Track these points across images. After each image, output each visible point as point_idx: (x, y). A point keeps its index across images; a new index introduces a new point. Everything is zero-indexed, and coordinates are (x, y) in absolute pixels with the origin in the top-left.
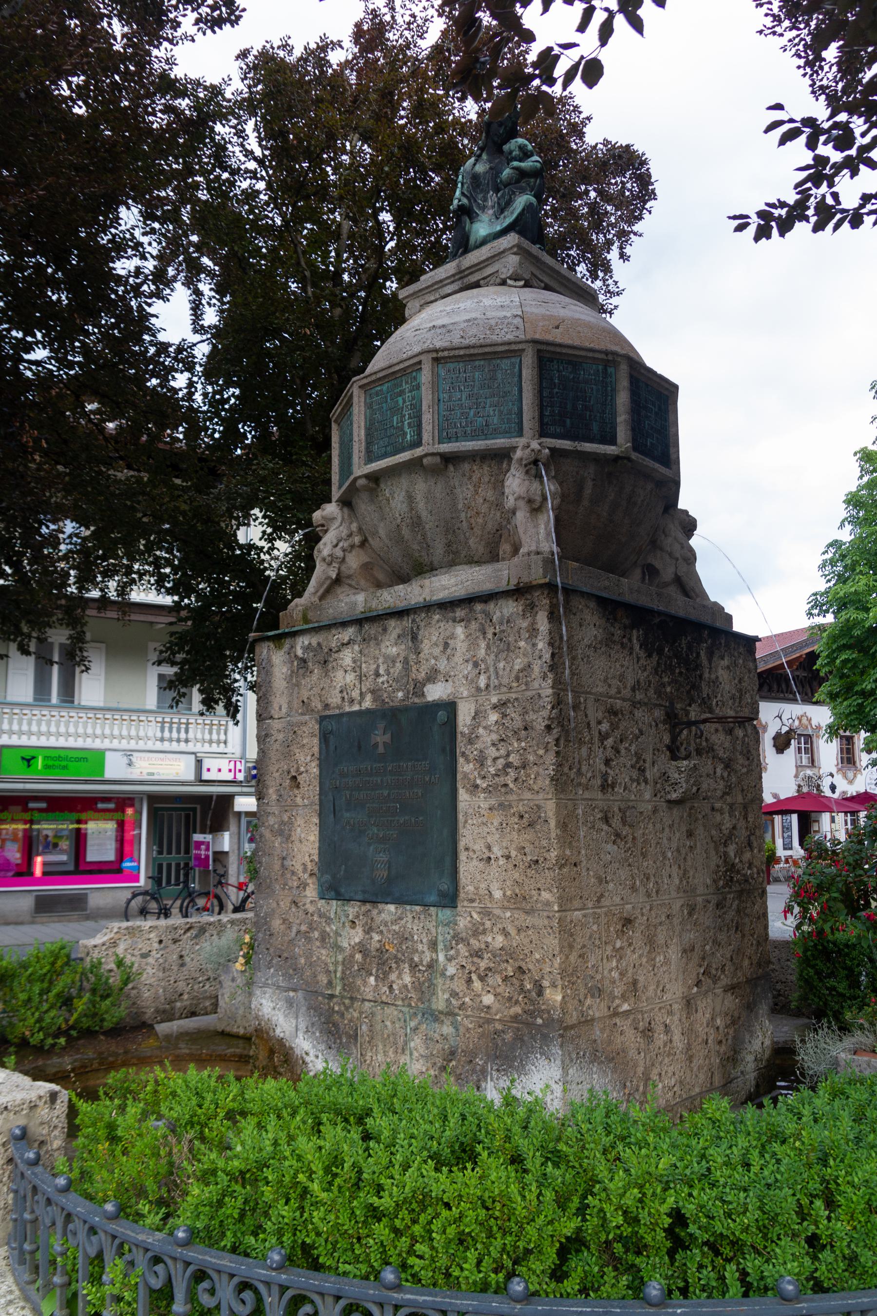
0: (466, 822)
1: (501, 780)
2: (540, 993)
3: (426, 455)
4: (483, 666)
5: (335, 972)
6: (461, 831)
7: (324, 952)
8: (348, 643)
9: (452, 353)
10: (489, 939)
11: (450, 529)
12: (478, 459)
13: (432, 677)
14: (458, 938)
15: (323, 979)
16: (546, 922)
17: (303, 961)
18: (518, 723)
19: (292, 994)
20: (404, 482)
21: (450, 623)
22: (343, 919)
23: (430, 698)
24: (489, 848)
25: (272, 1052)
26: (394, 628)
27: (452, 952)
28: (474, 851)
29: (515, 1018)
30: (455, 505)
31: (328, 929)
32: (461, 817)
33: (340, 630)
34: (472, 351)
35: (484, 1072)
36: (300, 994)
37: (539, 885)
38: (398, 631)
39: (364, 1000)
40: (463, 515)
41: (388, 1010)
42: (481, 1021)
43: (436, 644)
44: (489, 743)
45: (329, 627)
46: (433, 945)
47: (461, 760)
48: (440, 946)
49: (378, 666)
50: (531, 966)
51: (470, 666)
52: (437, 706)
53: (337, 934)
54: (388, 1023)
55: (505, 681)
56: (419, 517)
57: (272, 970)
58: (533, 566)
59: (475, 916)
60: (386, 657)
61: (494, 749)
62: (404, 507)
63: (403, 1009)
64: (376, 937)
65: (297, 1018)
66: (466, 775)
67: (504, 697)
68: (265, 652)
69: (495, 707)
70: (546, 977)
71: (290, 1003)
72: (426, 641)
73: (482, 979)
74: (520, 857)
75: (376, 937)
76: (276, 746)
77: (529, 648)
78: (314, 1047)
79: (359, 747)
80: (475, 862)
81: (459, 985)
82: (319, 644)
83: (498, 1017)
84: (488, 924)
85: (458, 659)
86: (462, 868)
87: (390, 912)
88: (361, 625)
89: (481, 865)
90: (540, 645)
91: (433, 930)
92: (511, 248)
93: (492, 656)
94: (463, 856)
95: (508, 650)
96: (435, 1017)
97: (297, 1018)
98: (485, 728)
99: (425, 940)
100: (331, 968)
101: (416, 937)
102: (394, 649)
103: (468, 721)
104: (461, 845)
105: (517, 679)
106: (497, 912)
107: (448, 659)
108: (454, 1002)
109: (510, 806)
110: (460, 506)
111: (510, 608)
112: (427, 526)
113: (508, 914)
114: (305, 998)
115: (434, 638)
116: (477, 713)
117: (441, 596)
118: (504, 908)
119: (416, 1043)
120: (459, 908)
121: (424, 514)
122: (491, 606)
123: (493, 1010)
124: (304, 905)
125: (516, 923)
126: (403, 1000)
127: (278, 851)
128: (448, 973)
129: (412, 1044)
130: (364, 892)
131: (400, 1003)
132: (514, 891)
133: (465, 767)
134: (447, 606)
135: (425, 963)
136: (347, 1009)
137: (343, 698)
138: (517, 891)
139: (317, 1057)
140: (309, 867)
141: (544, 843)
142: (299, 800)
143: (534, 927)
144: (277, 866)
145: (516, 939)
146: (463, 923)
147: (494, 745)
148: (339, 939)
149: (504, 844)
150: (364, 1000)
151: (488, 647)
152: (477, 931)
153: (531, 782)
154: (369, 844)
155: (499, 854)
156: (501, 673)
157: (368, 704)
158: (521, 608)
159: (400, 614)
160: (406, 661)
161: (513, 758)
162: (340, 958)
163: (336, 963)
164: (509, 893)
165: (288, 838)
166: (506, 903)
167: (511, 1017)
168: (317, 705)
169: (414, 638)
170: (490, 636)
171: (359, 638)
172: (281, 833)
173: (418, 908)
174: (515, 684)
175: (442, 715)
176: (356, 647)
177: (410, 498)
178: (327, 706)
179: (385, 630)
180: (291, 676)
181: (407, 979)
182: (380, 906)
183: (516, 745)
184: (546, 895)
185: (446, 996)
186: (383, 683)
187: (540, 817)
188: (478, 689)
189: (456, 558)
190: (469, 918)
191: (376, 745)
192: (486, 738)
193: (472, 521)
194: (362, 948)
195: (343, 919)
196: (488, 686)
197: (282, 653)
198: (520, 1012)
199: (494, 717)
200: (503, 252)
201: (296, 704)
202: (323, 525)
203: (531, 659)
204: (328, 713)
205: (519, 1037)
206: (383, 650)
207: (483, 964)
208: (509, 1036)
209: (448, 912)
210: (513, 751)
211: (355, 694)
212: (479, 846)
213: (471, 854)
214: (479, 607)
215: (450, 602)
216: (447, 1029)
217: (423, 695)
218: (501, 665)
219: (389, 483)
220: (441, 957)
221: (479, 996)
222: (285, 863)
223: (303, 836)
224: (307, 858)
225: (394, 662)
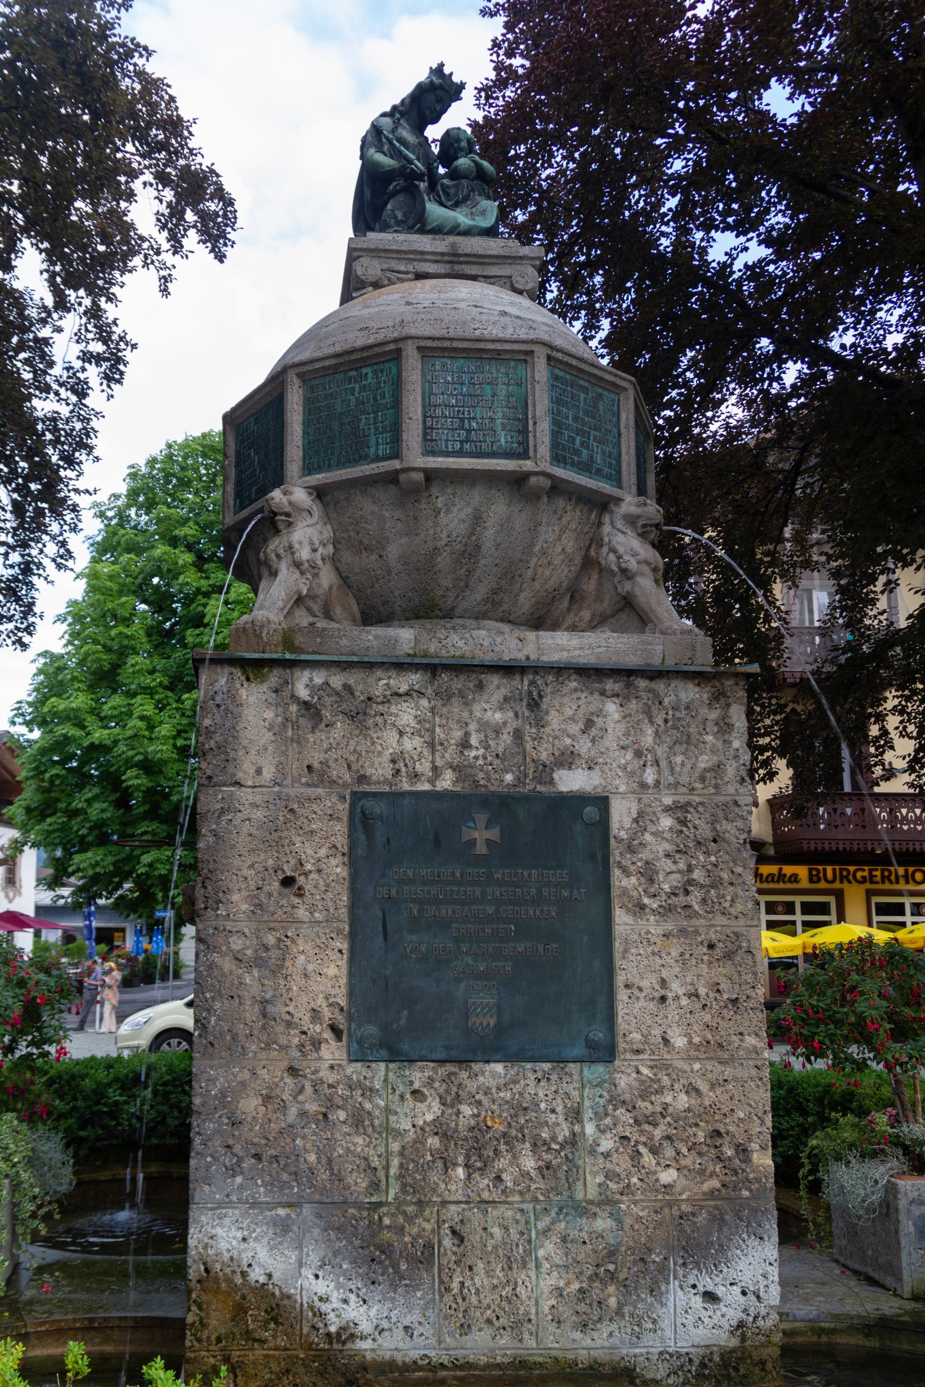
0: (626, 951)
1: (682, 900)
2: (747, 1160)
3: (537, 474)
4: (649, 757)
5: (387, 1168)
6: (618, 962)
7: (359, 1140)
8: (407, 694)
9: (566, 359)
10: (669, 1099)
11: (510, 574)
12: (574, 499)
13: (567, 759)
14: (616, 1101)
15: (359, 1182)
16: (754, 1072)
17: (312, 1158)
18: (705, 832)
19: (281, 1212)
20: (477, 496)
21: (596, 696)
22: (401, 1088)
23: (563, 788)
24: (663, 983)
25: (240, 1310)
26: (498, 687)
27: (608, 1121)
28: (640, 989)
29: (711, 1194)
30: (531, 545)
31: (368, 1106)
32: (618, 946)
33: (393, 673)
34: (583, 366)
35: (662, 1269)
36: (307, 1210)
37: (742, 1029)
38: (503, 691)
39: (444, 1203)
40: (534, 561)
41: (493, 1212)
42: (658, 1205)
43: (572, 719)
44: (661, 854)
45: (370, 666)
46: (575, 1115)
47: (616, 873)
48: (588, 1114)
49: (467, 734)
50: (732, 1128)
51: (629, 755)
52: (578, 800)
53: (388, 1111)
54: (496, 1231)
55: (684, 779)
56: (478, 547)
57: (239, 1180)
58: (699, 648)
59: (645, 1071)
60: (483, 726)
61: (669, 862)
62: (463, 528)
63: (524, 1206)
64: (467, 1110)
65: (300, 1247)
66: (625, 892)
67: (683, 800)
68: (223, 681)
69: (667, 809)
70: (755, 1138)
71: (283, 1227)
72: (553, 713)
73: (654, 1151)
74: (712, 995)
75: (467, 1110)
76: (246, 828)
77: (720, 745)
78: (338, 1286)
79: (437, 843)
80: (642, 1003)
81: (622, 1163)
82: (347, 687)
83: (684, 1197)
84: (666, 1081)
85: (610, 741)
86: (621, 1010)
87: (494, 1074)
88: (434, 675)
89: (652, 1006)
90: (736, 744)
91: (575, 1094)
92: (533, 258)
93: (665, 747)
94: (622, 995)
96: (583, 1210)
97: (300, 1247)
98: (653, 834)
99: (560, 1109)
100: (375, 1162)
101: (543, 1106)
102: (498, 716)
103: (627, 822)
104: (620, 979)
105: (702, 779)
106: (680, 1064)
108: (612, 1186)
109: (697, 932)
110: (537, 549)
111: (689, 692)
112: (483, 561)
113: (697, 1066)
114: (319, 1216)
115: (569, 712)
116: (641, 814)
117: (555, 657)
118: (691, 1059)
119: (548, 1249)
120: (617, 1063)
121: (488, 546)
122: (660, 686)
123: (678, 1188)
124: (316, 1072)
125: (710, 1076)
126: (521, 1193)
127: (256, 990)
128: (601, 1149)
129: (541, 1253)
130: (447, 1048)
131: (517, 1198)
132: (704, 1037)
133: (623, 882)
134: (591, 674)
135: (560, 1139)
136: (410, 1219)
137: (398, 771)
138: (709, 1037)
139: (345, 1301)
140: (327, 1013)
141: (749, 978)
142: (302, 913)
143: (736, 1079)
144: (251, 1012)
145: (709, 1097)
146: (625, 1081)
147: (668, 856)
148: (392, 1118)
149: (688, 980)
150: (444, 1203)
151: (657, 734)
152: (647, 1090)
153: (727, 905)
154: (458, 980)
155: (681, 992)
156: (678, 769)
157: (446, 782)
158: (705, 696)
159: (508, 670)
160: (518, 735)
161: (697, 875)
162: (395, 1146)
163: (387, 1157)
164: (696, 1040)
165: (277, 971)
166: (692, 1053)
167: (704, 1194)
168: (338, 772)
169: (534, 704)
170: (660, 721)
171: (430, 691)
172: (259, 962)
173: (546, 1066)
174: (698, 785)
175: (590, 812)
176: (424, 702)
177: (477, 519)
178: (362, 779)
179: (480, 686)
180: (284, 726)
181: (529, 1163)
182: (476, 1067)
183: (702, 858)
184: (751, 1040)
185: (600, 1179)
186: (476, 758)
187: (740, 947)
188: (643, 786)
189: (494, 610)
190: (634, 1075)
191: (473, 843)
192: (656, 847)
193: (540, 570)
194: (440, 1129)
195: (401, 1088)
196: (658, 782)
197: (264, 687)
198: (718, 1185)
199: (666, 822)
200: (521, 258)
201: (295, 768)
202: (288, 515)
203: (722, 758)
204: (367, 788)
205: (718, 1220)
207: (658, 1133)
208: (702, 1218)
209: (600, 1069)
210: (696, 866)
211: (424, 767)
212: (649, 982)
213: (636, 992)
214: (642, 683)
215: (610, 670)
216: (603, 1223)
217: (552, 782)
218: (679, 759)
219: (449, 491)
220: (590, 1129)
221: (655, 1173)
222: (270, 1008)
223: (310, 967)
224: (321, 1001)
225: (497, 732)
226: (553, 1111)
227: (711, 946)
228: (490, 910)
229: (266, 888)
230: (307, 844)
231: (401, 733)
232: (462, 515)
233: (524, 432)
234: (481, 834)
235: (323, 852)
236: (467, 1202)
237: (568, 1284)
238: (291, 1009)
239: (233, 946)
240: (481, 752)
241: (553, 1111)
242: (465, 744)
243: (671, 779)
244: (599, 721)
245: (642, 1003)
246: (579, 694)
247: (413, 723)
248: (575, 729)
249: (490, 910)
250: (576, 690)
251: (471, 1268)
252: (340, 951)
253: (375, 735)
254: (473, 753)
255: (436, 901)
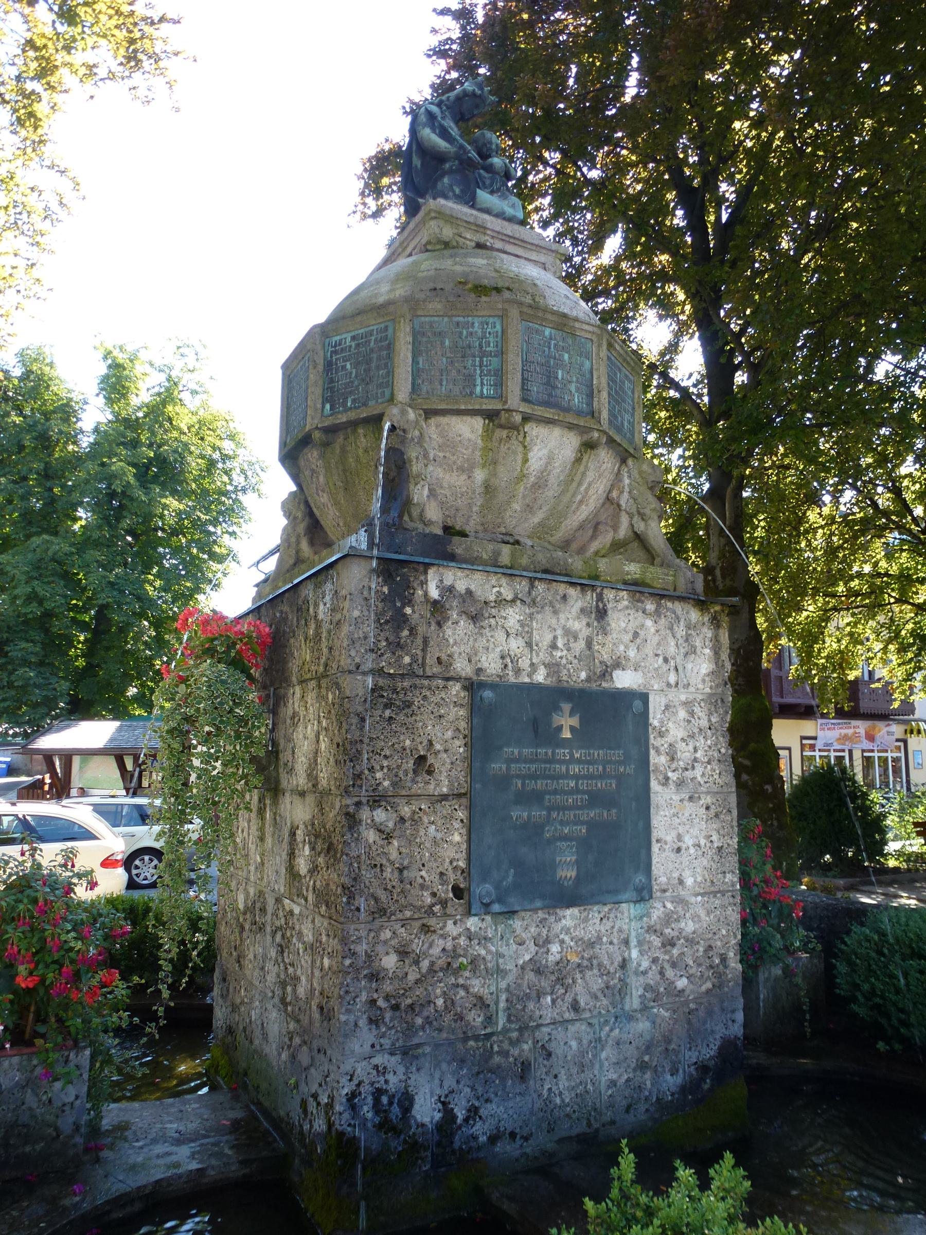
16: (731, 900)
21: (640, 613)
38: (579, 604)
41: (572, 1029)
47: (652, 752)
48: (633, 942)
49: (555, 638)
60: (568, 632)
67: (691, 697)
85: (649, 650)
94: (655, 848)
95: (695, 653)
99: (615, 941)
101: (605, 939)
104: (655, 835)
107: (638, 648)
129: (604, 1055)
133: (657, 760)
137: (506, 666)
152: (669, 919)
157: (540, 677)
164: (699, 879)
175: (637, 704)
186: (561, 658)
188: (669, 685)
192: (676, 732)
206: (562, 621)
212: (670, 837)
220: (635, 953)
223: (439, 836)
226: (611, 943)
227: (708, 808)
228: (572, 784)
229: (404, 767)
230: (437, 728)
231: (508, 634)
232: (540, 454)
233: (591, 395)
234: (566, 722)
235: (449, 734)
236: (553, 1024)
237: (620, 1076)
238: (423, 873)
239: (377, 819)
240: (565, 652)
241: (611, 943)
242: (554, 646)
243: (685, 682)
244: (642, 633)
245: (667, 853)
246: (629, 611)
247: (517, 626)
248: (627, 637)
249: (572, 784)
250: (627, 608)
251: (556, 1076)
252: (462, 821)
253: (489, 634)
254: (559, 654)
255: (534, 777)
